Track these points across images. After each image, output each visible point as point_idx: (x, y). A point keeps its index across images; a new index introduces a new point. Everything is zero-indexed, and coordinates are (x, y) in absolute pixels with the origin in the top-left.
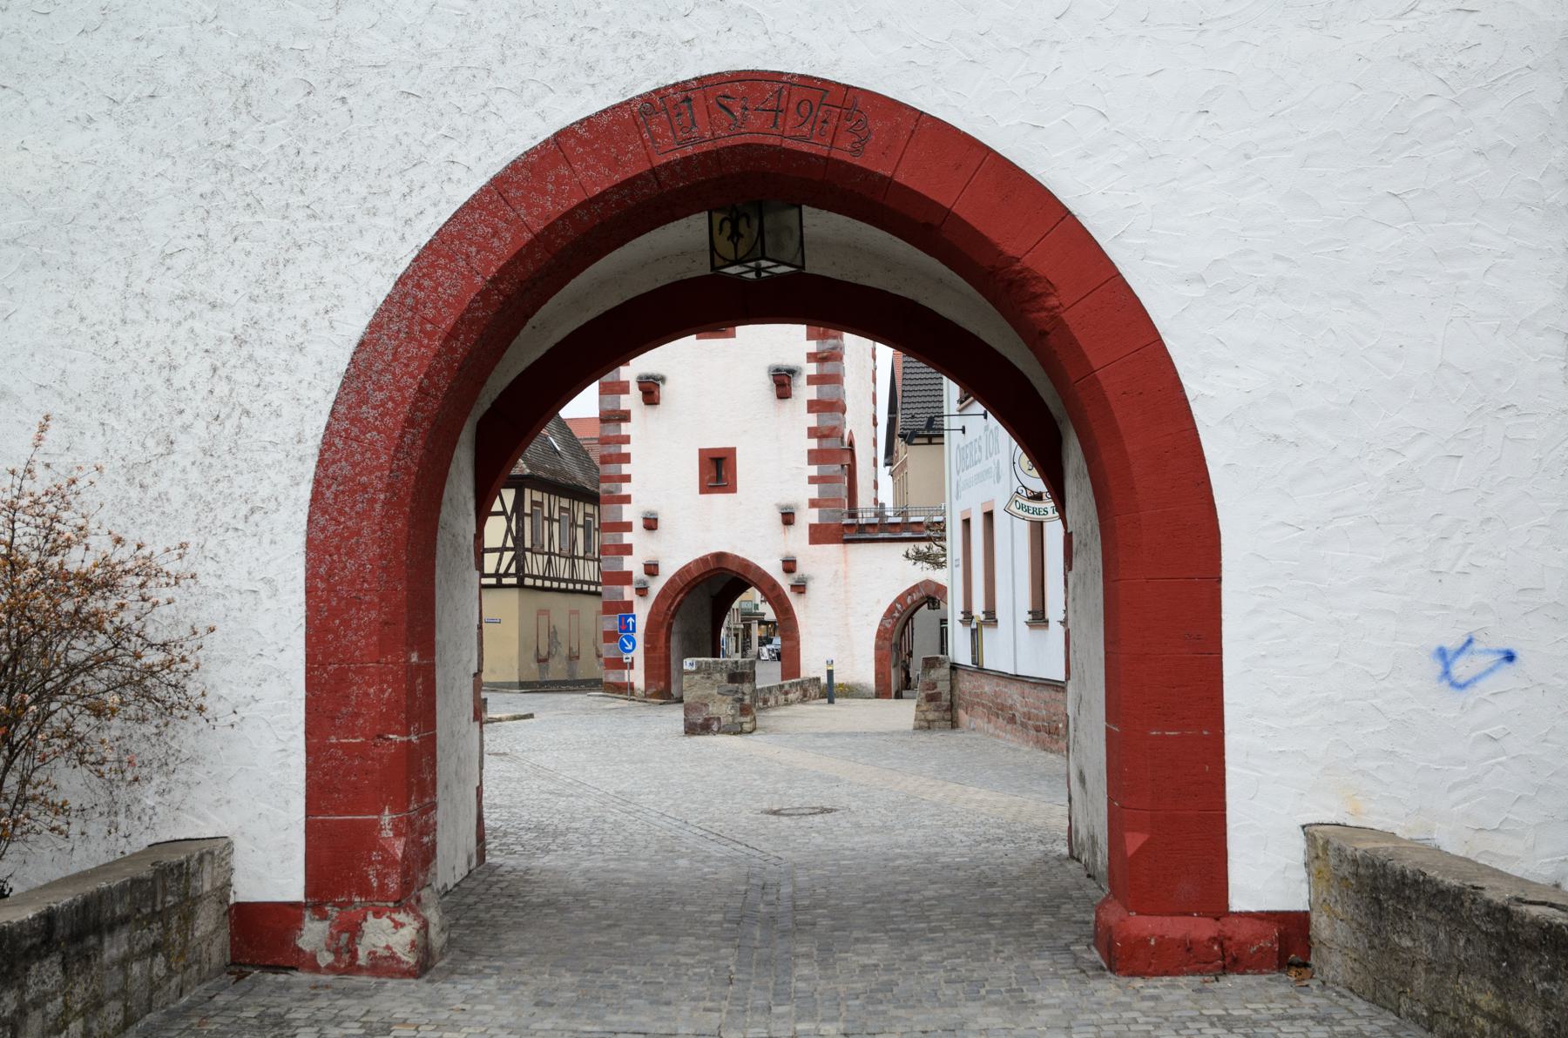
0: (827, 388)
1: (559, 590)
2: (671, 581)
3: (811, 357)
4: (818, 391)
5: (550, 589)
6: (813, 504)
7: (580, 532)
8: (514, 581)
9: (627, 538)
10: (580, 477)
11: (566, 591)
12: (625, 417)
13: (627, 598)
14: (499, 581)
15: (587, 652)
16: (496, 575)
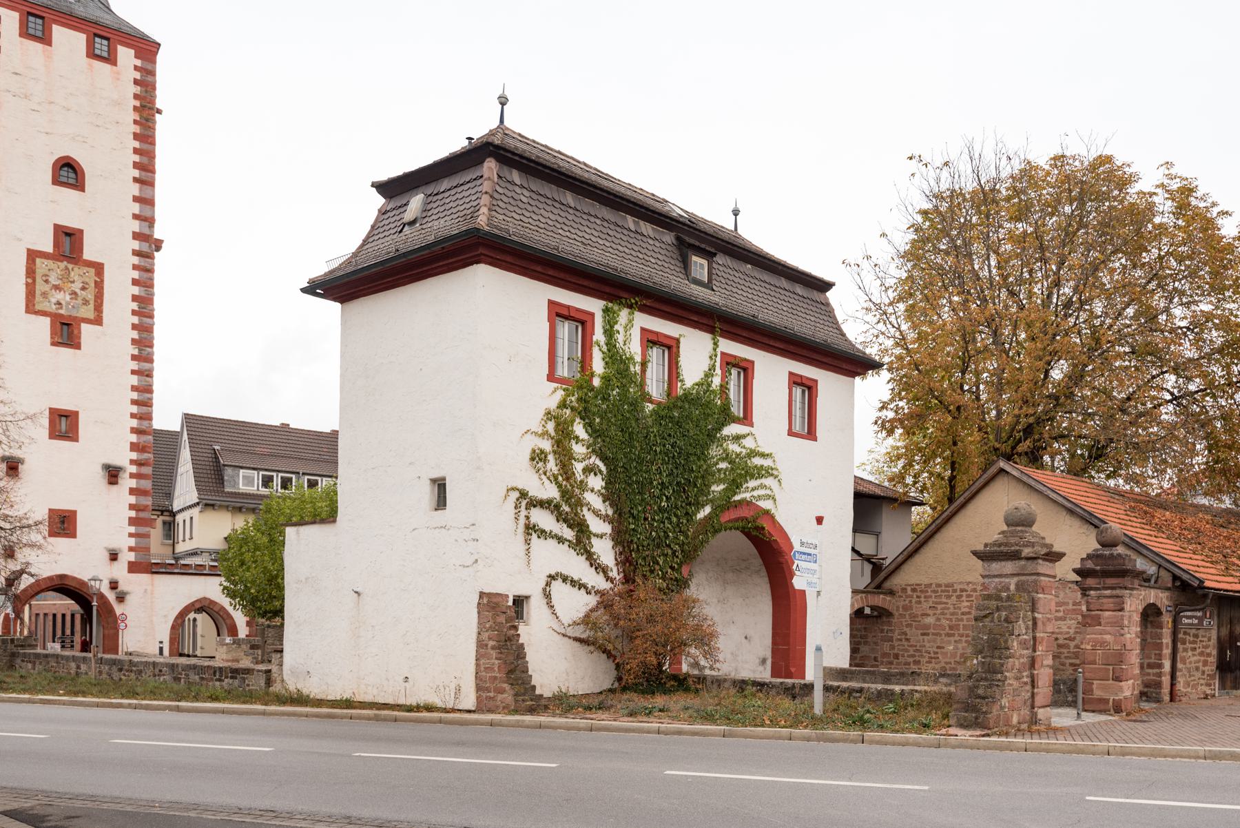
3: (132, 462)
4: (137, 483)
6: (131, 549)
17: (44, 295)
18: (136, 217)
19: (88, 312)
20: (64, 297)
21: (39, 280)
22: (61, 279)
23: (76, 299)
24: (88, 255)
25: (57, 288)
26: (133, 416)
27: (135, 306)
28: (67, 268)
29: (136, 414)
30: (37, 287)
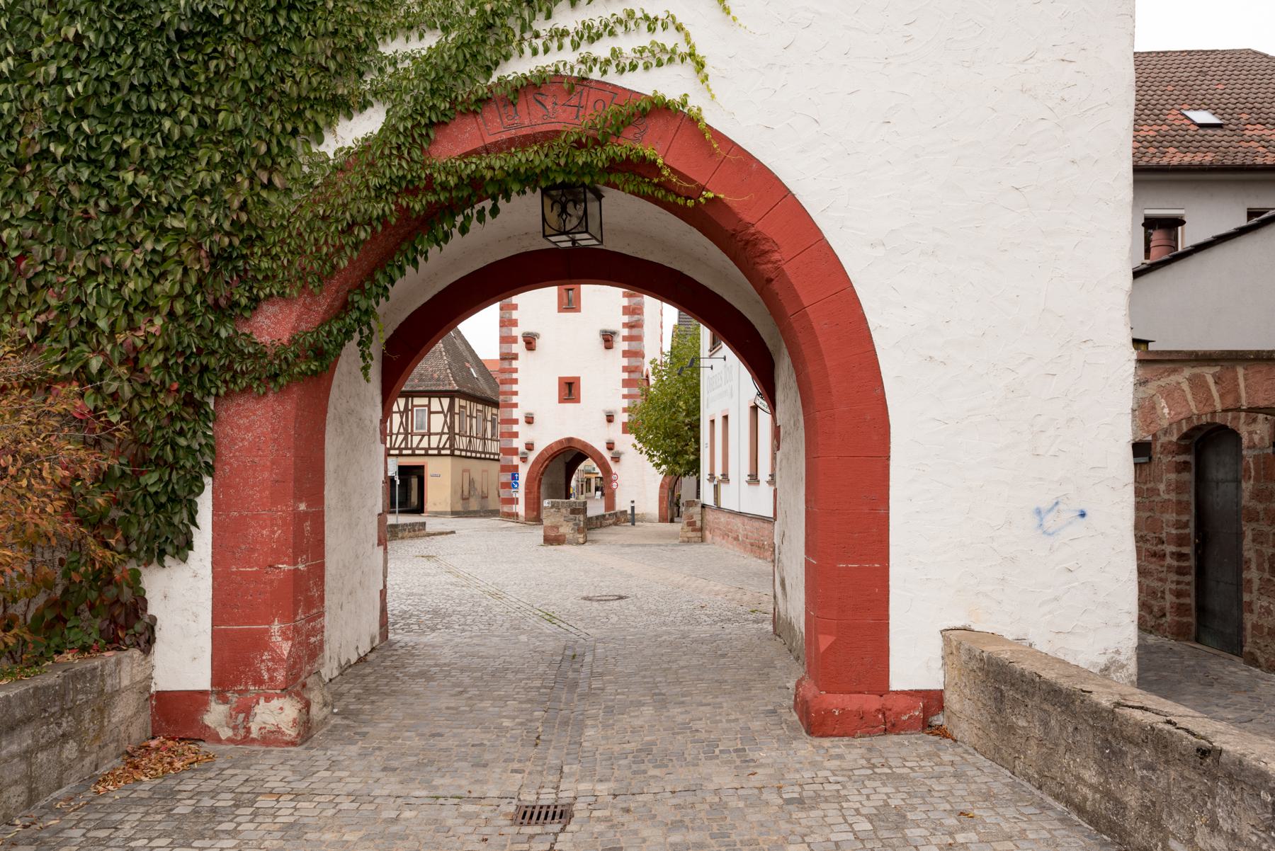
0: (633, 343)
1: (476, 458)
2: (541, 454)
3: (625, 325)
5: (470, 457)
6: (625, 410)
7: (489, 425)
8: (448, 452)
9: (515, 428)
10: (489, 393)
11: (480, 458)
12: (515, 357)
13: (515, 463)
14: (439, 452)
15: (493, 495)
16: (438, 448)
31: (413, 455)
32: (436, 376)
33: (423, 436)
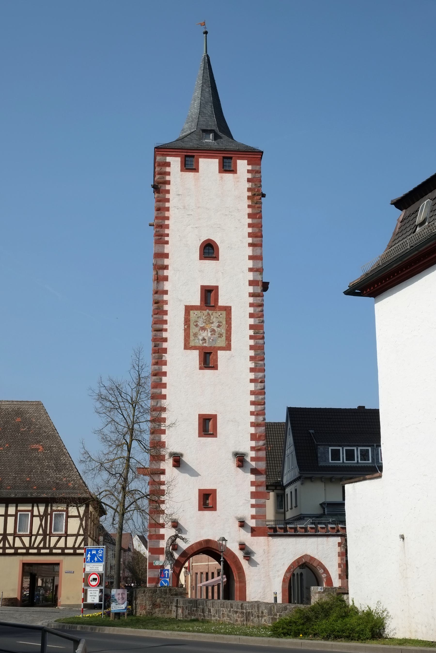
3: (252, 449)
6: (253, 517)
14: (75, 551)
16: (73, 548)
17: (195, 335)
18: (250, 270)
19: (221, 342)
20: (206, 334)
21: (192, 325)
22: (205, 322)
23: (215, 335)
24: (222, 302)
25: (203, 329)
26: (252, 413)
27: (251, 332)
28: (208, 314)
29: (254, 412)
30: (191, 331)
31: (51, 554)
32: (71, 484)
33: (60, 537)
